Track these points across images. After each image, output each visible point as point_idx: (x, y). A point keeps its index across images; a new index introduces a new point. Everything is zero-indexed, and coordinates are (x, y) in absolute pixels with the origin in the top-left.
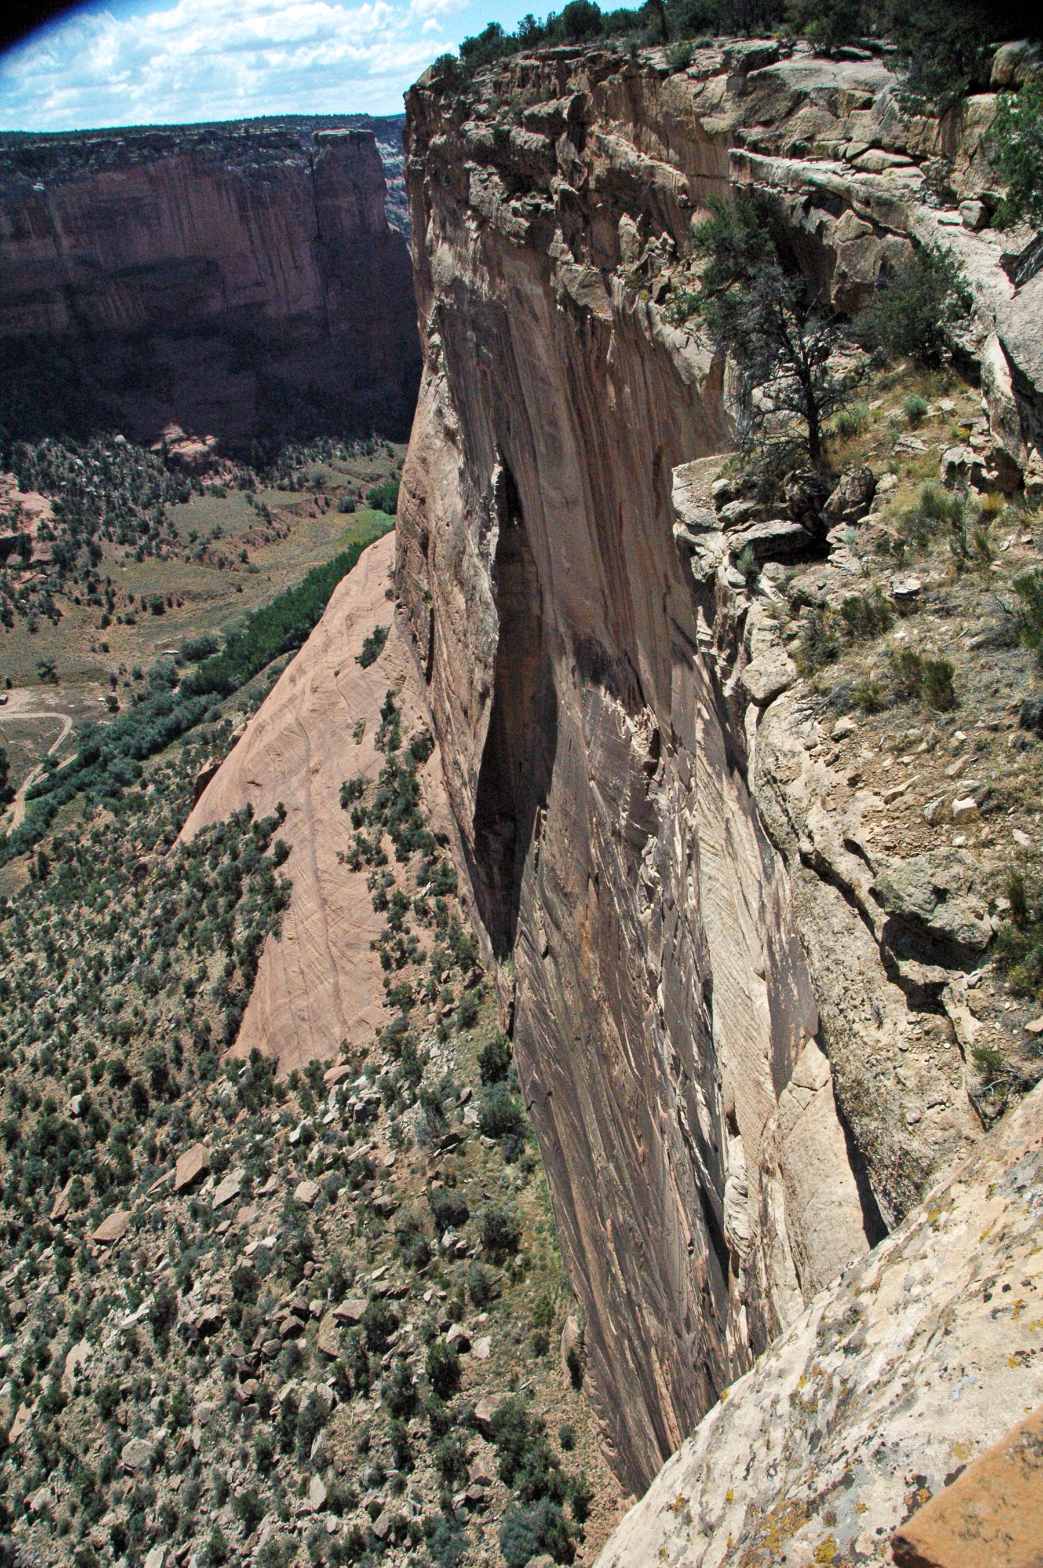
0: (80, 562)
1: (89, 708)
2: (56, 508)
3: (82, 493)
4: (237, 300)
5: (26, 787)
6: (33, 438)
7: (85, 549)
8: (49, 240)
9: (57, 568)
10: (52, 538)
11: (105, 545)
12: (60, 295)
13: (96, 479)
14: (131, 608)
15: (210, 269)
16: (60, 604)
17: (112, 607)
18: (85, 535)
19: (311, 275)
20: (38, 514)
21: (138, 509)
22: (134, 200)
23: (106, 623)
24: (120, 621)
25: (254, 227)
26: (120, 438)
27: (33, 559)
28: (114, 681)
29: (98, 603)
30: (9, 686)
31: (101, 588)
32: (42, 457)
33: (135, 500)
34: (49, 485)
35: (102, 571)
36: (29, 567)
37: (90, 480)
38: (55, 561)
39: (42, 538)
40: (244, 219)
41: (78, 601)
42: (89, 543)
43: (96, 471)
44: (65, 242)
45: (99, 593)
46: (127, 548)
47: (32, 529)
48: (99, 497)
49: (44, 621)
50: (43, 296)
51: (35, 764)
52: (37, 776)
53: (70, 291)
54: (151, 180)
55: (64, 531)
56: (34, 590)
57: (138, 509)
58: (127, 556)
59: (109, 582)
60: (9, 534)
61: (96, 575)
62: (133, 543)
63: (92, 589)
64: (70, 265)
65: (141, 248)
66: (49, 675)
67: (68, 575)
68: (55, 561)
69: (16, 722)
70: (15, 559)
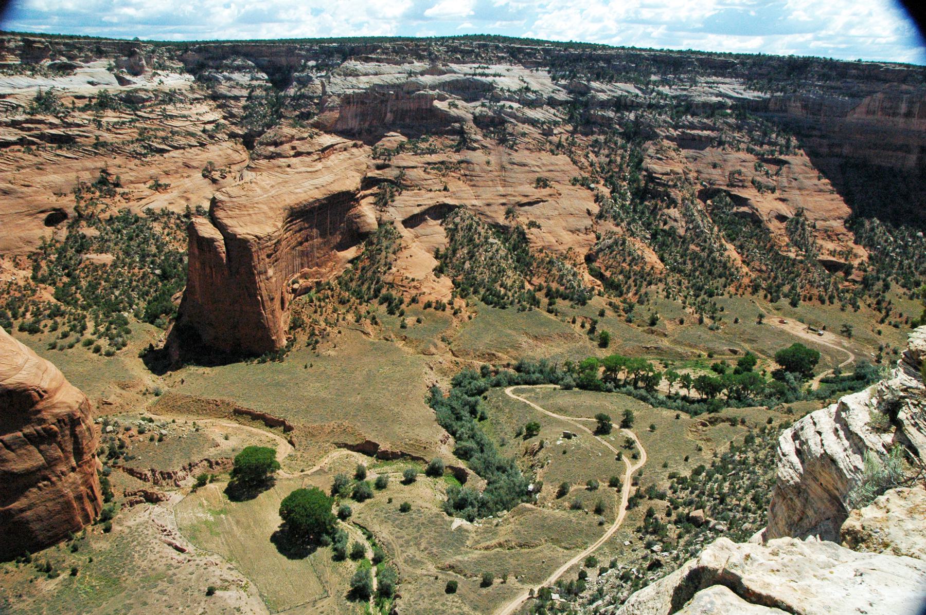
0: (875, 288)
1: (865, 356)
2: (870, 258)
3: (887, 255)
5: (822, 376)
6: (870, 217)
7: (881, 283)
9: (861, 286)
10: (865, 271)
11: (893, 284)
12: (916, 151)
13: (898, 250)
14: (898, 320)
16: (860, 303)
17: (887, 315)
18: (884, 276)
20: (860, 257)
21: (917, 274)
23: (882, 321)
24: (890, 324)
26: (920, 234)
27: (849, 278)
28: (881, 349)
29: (880, 310)
30: (824, 329)
31: (884, 305)
32: (872, 229)
33: (916, 268)
34: (870, 244)
35: (888, 296)
36: (847, 280)
37: (894, 250)
38: (862, 283)
39: (859, 269)
41: (869, 306)
42: (884, 280)
43: (899, 247)
45: (881, 307)
46: (905, 290)
47: (855, 263)
48: (896, 260)
49: (850, 308)
50: (906, 148)
51: (829, 368)
52: (829, 373)
55: (873, 270)
56: (847, 291)
57: (917, 274)
58: (904, 294)
59: (890, 303)
60: (842, 261)
61: (884, 297)
62: (909, 289)
63: (878, 303)
66: (847, 332)
67: (866, 292)
68: (862, 283)
69: (824, 346)
70: (841, 274)
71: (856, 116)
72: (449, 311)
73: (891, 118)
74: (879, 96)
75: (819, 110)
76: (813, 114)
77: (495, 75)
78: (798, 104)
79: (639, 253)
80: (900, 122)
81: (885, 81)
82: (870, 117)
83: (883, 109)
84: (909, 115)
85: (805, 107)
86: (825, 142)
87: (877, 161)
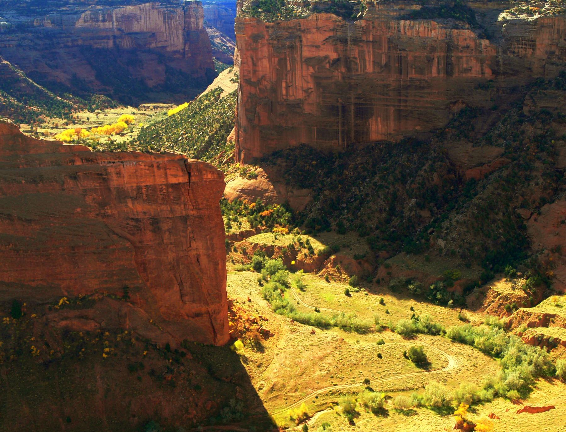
4: (159, 45)
8: (111, 23)
12: (112, 38)
15: (153, 35)
19: (181, 40)
22: (135, 14)
25: (167, 25)
40: (164, 22)
44: (115, 24)
50: (108, 38)
53: (115, 37)
54: (140, 10)
64: (115, 30)
65: (136, 27)
71: (80, 24)
74: (88, 12)
76: (59, 25)
78: (49, 21)
80: (101, 24)
82: (86, 24)
84: (104, 21)
85: (53, 22)
87: (96, 46)
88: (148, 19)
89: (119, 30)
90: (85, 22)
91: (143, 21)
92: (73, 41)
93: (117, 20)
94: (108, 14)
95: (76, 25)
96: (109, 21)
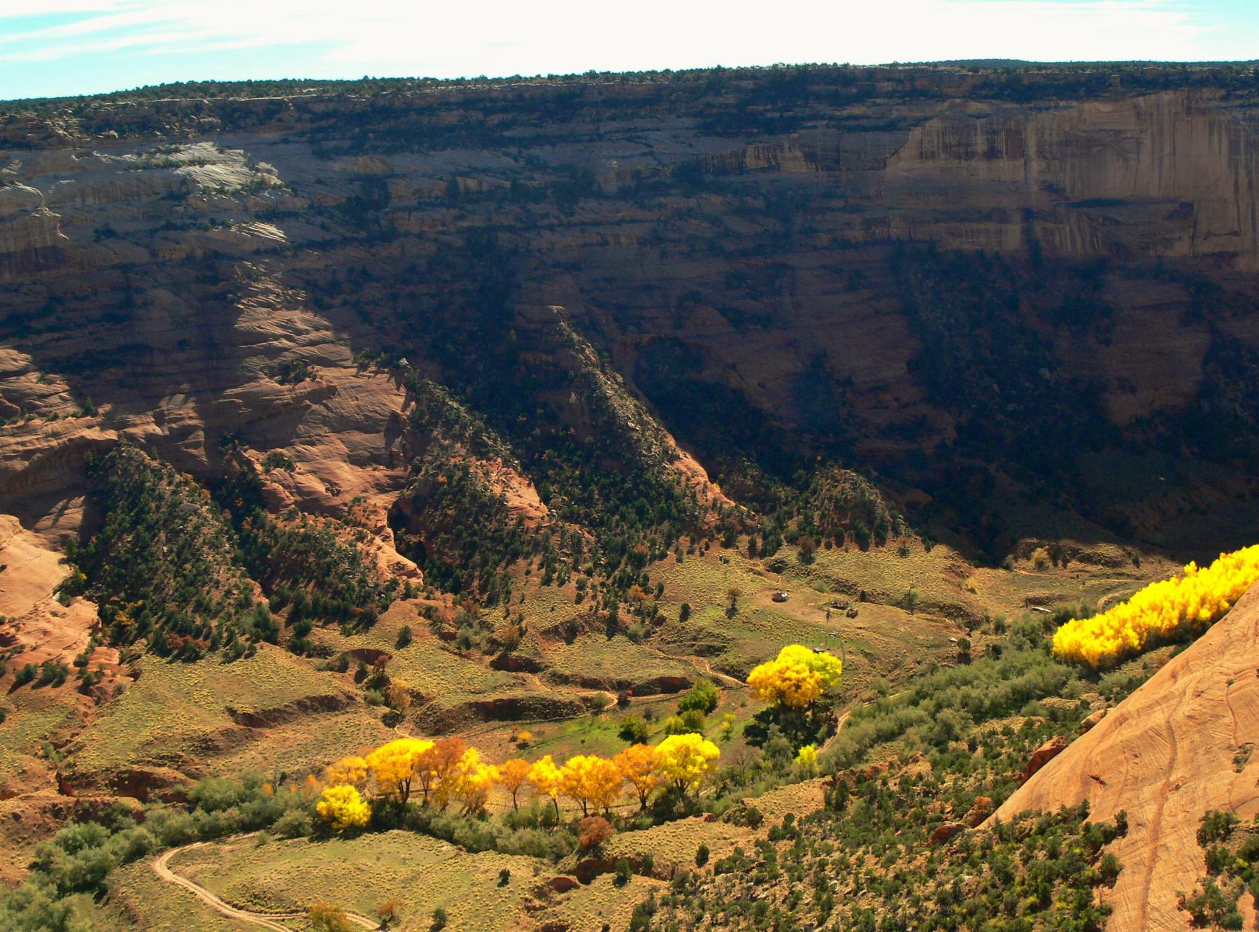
4: (1205, 247)
12: (1017, 217)
15: (1185, 211)
25: (1242, 172)
40: (1233, 164)
50: (1002, 216)
64: (1035, 188)
65: (1114, 180)
71: (903, 167)
72: (72, 682)
73: (964, 163)
74: (935, 124)
75: (837, 162)
76: (828, 168)
77: (192, 163)
78: (799, 154)
79: (497, 490)
81: (942, 98)
83: (946, 147)
84: (992, 154)
85: (810, 157)
86: (856, 218)
87: (955, 244)
88: (1167, 150)
89: (1050, 188)
90: (922, 156)
91: (1146, 157)
92: (868, 224)
93: (1041, 154)
94: (1008, 132)
95: (890, 171)
96: (1013, 157)
